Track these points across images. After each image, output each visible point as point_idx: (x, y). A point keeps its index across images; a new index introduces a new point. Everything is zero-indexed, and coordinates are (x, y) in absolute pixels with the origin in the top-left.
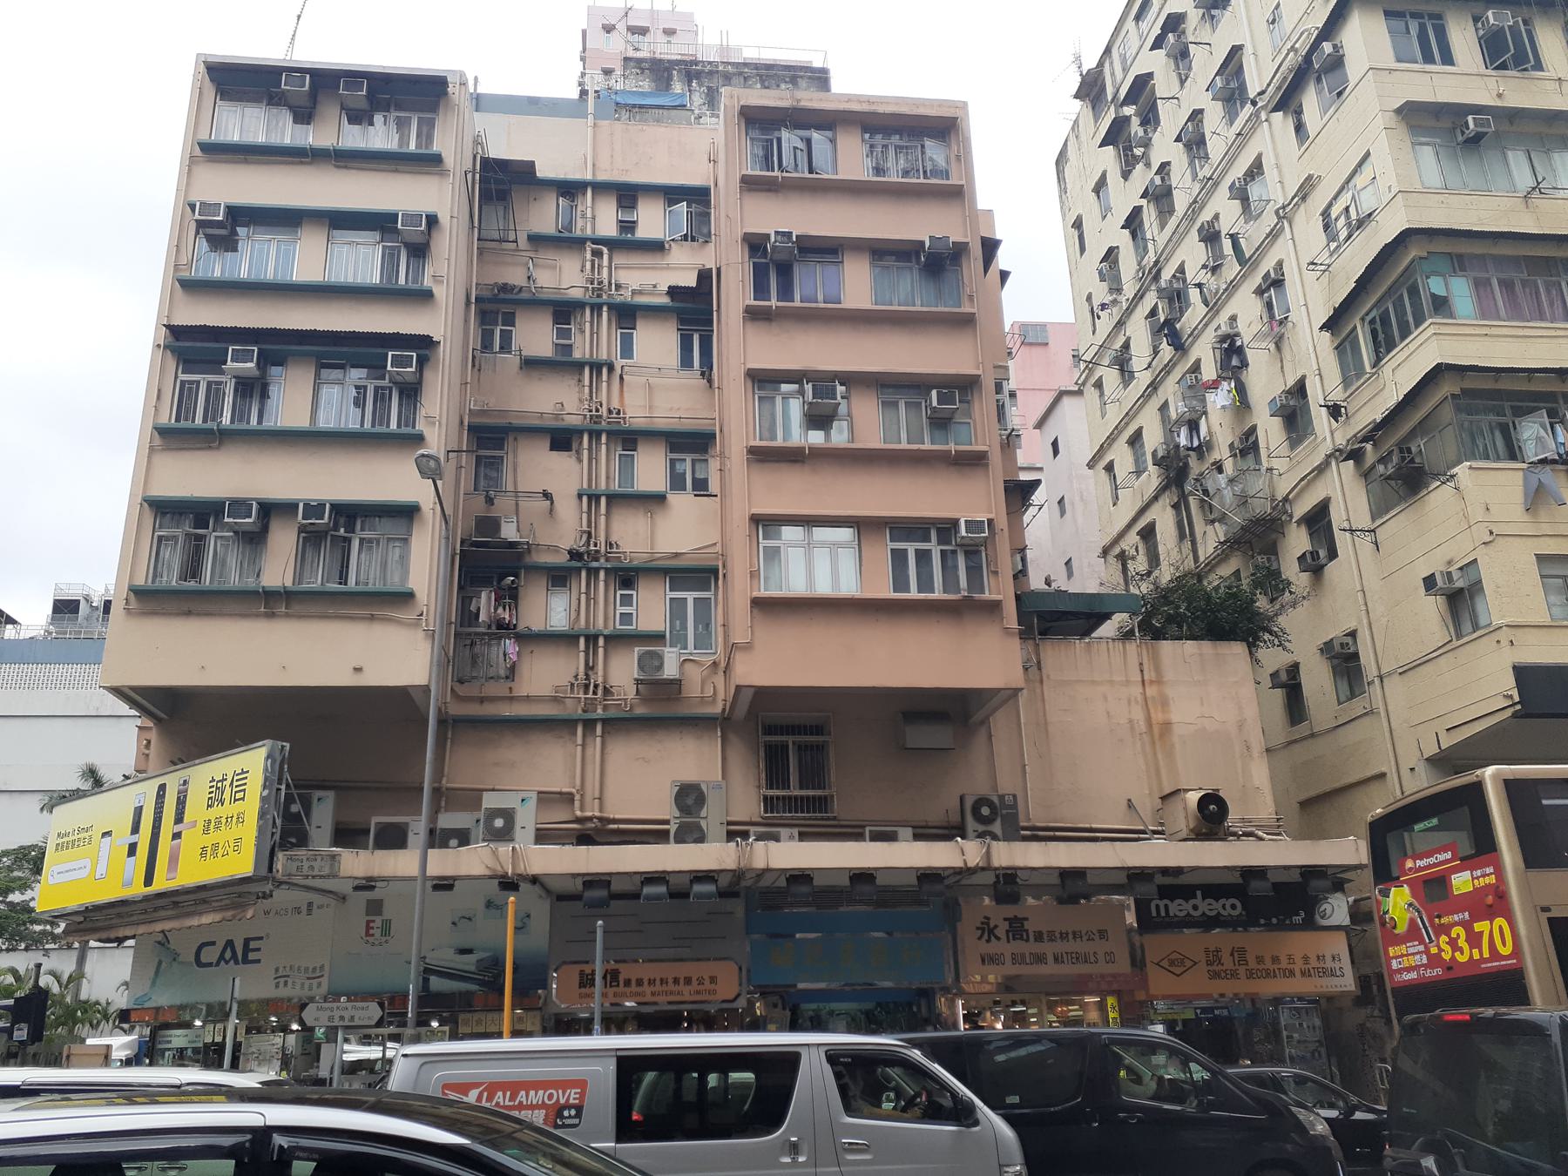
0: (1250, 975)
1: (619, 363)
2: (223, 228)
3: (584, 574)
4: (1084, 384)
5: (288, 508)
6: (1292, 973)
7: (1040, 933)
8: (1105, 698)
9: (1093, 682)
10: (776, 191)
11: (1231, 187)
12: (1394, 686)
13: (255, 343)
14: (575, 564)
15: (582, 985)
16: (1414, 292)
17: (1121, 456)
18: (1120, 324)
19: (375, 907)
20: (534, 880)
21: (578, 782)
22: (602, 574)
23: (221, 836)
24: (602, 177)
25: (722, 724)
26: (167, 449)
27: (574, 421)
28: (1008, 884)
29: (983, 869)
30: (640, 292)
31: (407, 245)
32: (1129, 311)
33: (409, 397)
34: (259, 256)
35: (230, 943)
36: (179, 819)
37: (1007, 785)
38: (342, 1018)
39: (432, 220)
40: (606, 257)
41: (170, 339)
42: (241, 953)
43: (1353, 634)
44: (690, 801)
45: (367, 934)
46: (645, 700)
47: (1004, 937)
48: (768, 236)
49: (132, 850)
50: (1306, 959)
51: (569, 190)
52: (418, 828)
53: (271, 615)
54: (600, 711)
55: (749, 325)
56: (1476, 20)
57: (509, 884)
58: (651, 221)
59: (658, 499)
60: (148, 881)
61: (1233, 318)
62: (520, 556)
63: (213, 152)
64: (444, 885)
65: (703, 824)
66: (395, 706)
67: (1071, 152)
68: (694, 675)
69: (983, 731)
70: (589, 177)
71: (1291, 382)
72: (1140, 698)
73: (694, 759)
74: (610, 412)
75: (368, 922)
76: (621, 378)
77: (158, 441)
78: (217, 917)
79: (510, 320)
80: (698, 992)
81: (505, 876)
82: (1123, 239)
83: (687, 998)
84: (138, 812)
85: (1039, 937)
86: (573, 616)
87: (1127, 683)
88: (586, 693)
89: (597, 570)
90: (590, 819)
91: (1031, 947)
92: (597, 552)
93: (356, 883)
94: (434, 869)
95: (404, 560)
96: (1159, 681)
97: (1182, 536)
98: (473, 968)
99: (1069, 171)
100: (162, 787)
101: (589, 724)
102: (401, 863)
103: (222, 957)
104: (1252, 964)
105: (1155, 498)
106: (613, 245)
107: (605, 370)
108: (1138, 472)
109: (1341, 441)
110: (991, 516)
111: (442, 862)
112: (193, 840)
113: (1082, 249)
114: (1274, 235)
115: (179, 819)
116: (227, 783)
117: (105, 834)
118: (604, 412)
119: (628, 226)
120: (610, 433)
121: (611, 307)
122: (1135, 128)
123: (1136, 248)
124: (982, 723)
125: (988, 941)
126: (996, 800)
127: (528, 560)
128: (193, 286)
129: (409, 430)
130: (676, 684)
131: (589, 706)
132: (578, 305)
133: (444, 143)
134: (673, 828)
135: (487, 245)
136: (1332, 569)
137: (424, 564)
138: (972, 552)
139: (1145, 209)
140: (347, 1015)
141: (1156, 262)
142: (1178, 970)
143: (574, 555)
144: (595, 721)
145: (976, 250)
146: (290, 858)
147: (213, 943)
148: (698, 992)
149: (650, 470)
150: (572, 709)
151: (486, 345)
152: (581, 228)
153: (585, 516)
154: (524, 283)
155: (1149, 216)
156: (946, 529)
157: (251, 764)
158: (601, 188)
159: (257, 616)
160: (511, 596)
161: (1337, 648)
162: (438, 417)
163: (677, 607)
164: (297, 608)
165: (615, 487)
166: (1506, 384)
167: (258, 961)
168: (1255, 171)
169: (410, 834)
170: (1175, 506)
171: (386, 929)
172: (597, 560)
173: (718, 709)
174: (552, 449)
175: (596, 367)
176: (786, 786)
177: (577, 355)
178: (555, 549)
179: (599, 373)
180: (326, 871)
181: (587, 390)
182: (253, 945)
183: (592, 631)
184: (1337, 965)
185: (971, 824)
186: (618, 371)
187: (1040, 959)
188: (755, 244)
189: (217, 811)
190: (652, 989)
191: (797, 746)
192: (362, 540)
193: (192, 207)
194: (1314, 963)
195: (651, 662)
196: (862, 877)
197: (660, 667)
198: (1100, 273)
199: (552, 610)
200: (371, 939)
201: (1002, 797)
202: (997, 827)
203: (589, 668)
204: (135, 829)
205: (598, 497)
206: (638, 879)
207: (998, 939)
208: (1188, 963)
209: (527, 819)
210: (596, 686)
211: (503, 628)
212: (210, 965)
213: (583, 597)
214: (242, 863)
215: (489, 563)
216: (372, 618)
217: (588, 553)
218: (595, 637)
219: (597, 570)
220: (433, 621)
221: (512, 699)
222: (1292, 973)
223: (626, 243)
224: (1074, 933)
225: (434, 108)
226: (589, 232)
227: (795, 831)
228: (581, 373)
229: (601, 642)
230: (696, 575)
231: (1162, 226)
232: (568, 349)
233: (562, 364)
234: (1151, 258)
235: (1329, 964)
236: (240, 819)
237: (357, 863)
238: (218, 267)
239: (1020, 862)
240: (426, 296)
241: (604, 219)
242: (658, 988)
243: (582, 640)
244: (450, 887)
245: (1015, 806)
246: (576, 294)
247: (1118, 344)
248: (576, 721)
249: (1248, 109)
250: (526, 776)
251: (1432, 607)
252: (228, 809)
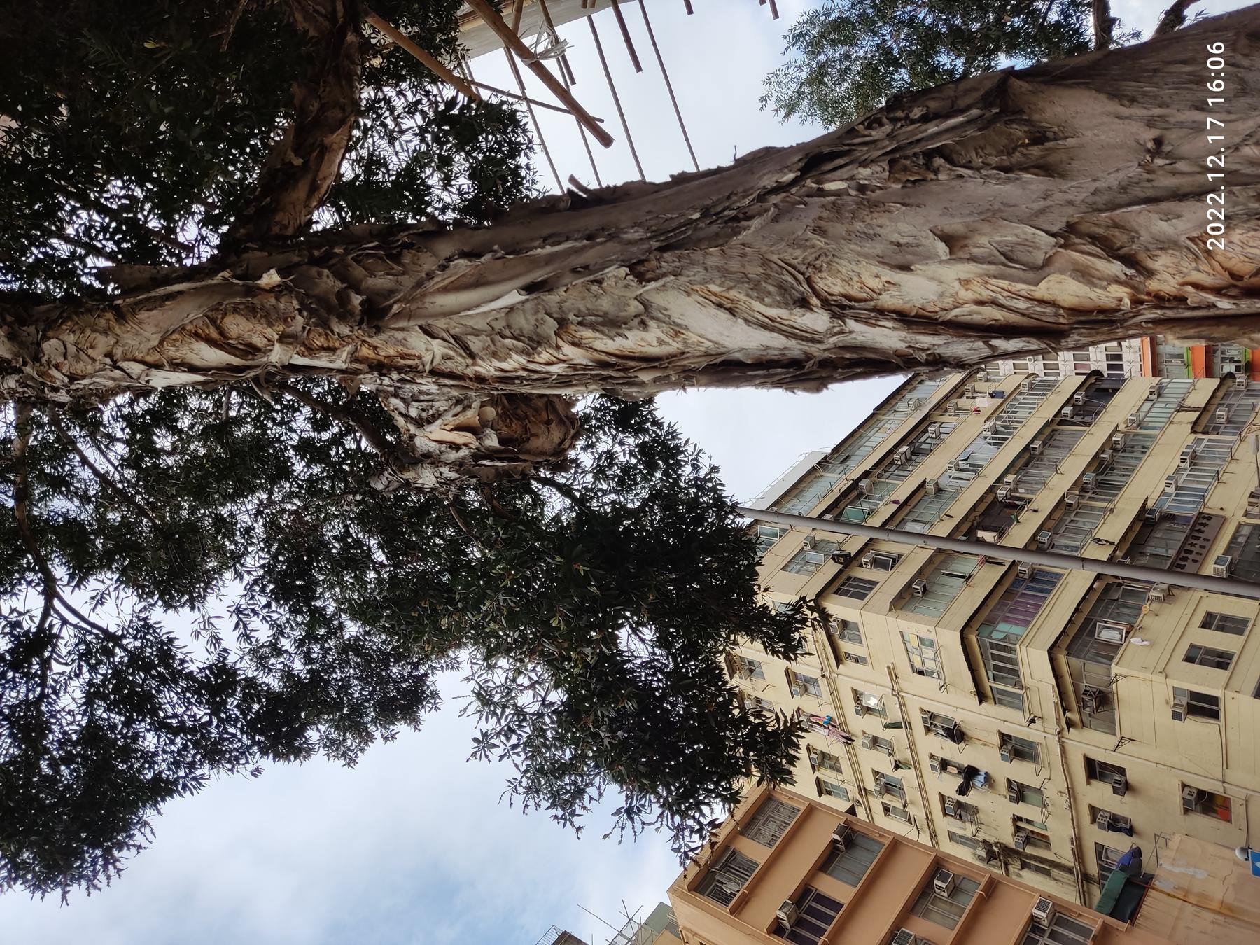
11: (858, 713)
12: (1232, 776)
16: (993, 646)
43: (1184, 786)
56: (861, 565)
61: (932, 756)
71: (997, 741)
97: (1047, 873)
109: (1053, 727)
114: (902, 705)
123: (837, 795)
136: (1131, 777)
139: (821, 777)
155: (827, 775)
161: (1192, 798)
166: (1073, 631)
168: (857, 695)
170: (1024, 866)
231: (839, 771)
249: (823, 683)
251: (1194, 726)
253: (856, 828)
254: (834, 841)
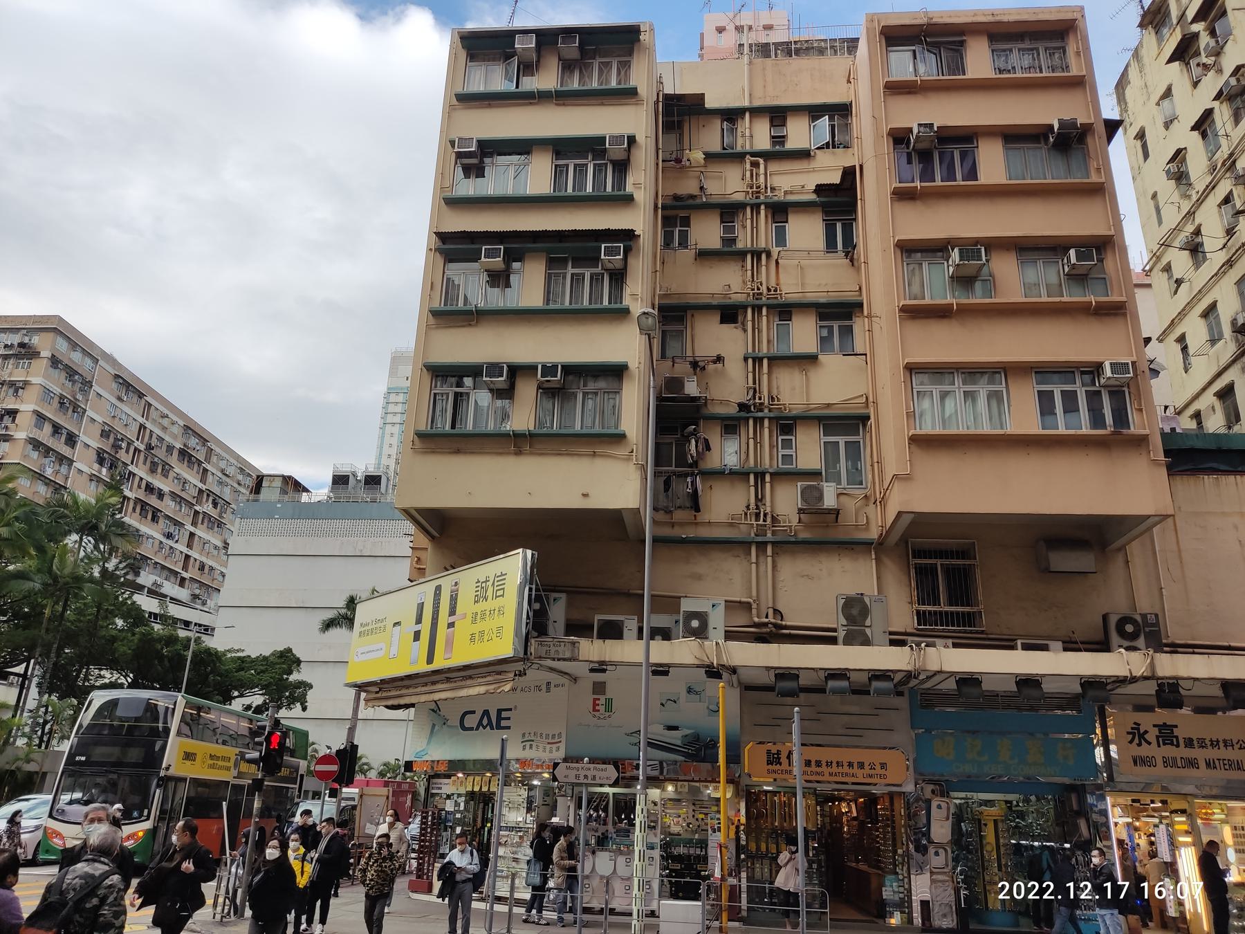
1: (775, 251)
2: (475, 158)
3: (751, 422)
4: (1151, 270)
5: (530, 369)
7: (1191, 740)
8: (1236, 527)
9: (1223, 513)
10: (915, 93)
13: (501, 243)
14: (743, 414)
15: (769, 763)
17: (1196, 330)
18: (1191, 214)
19: (599, 688)
20: (733, 670)
21: (754, 593)
22: (766, 422)
23: (488, 625)
24: (757, 103)
25: (877, 548)
26: (438, 327)
27: (740, 298)
28: (1170, 693)
29: (1146, 678)
30: (791, 193)
31: (611, 161)
32: (1200, 202)
33: (617, 280)
34: (501, 178)
35: (486, 713)
36: (452, 612)
37: (1145, 605)
38: (586, 777)
39: (632, 140)
40: (762, 167)
41: (439, 244)
42: (495, 720)
44: (855, 612)
45: (594, 710)
46: (808, 526)
48: (910, 130)
49: (417, 636)
51: (731, 116)
52: (631, 625)
53: (519, 453)
54: (769, 535)
55: (897, 205)
57: (713, 672)
58: (798, 134)
59: (812, 359)
60: (430, 660)
62: (698, 408)
63: (467, 100)
64: (661, 671)
65: (868, 631)
66: (610, 527)
67: (1133, 74)
68: (850, 505)
69: (1120, 558)
70: (746, 104)
73: (854, 576)
74: (769, 290)
75: (595, 700)
76: (777, 263)
77: (432, 320)
78: (482, 689)
79: (686, 222)
80: (871, 776)
81: (710, 666)
82: (1193, 142)
83: (826, 778)
84: (421, 607)
85: (1189, 743)
86: (743, 457)
88: (757, 519)
89: (762, 419)
90: (765, 625)
91: (1183, 752)
92: (761, 404)
93: (592, 665)
94: (654, 659)
95: (616, 412)
98: (679, 743)
99: (1129, 93)
100: (438, 588)
101: (762, 546)
102: (628, 650)
103: (480, 723)
105: (1234, 362)
106: (767, 156)
107: (764, 256)
108: (1213, 342)
110: (1134, 359)
111: (661, 652)
112: (464, 628)
113: (1146, 155)
115: (452, 612)
116: (490, 583)
117: (396, 624)
118: (764, 289)
119: (779, 140)
120: (769, 307)
121: (768, 206)
122: (1205, 40)
123: (1206, 146)
124: (1119, 550)
125: (1139, 745)
127: (705, 411)
128: (455, 203)
129: (618, 306)
130: (837, 512)
131: (761, 531)
132: (741, 206)
133: (639, 78)
134: (841, 634)
135: (673, 164)
137: (633, 410)
138: (1117, 394)
139: (1217, 111)
140: (590, 774)
141: (1231, 155)
143: (743, 407)
144: (766, 543)
145: (1101, 129)
146: (541, 644)
147: (473, 712)
148: (871, 776)
149: (804, 334)
150: (746, 531)
151: (668, 243)
152: (742, 145)
153: (750, 375)
154: (696, 192)
156: (1095, 369)
157: (513, 566)
158: (756, 112)
159: (509, 454)
162: (638, 295)
163: (830, 452)
165: (775, 351)
167: (509, 728)
169: (625, 630)
171: (609, 704)
172: (761, 410)
173: (874, 534)
174: (722, 322)
175: (756, 254)
176: (936, 602)
177: (740, 245)
179: (759, 259)
180: (568, 655)
181: (749, 273)
182: (504, 714)
183: (759, 469)
185: (1115, 638)
186: (775, 256)
188: (899, 138)
189: (483, 605)
190: (829, 769)
191: (948, 569)
192: (585, 394)
193: (452, 143)
195: (812, 496)
196: (1028, 683)
197: (821, 498)
198: (1168, 172)
199: (728, 453)
200: (597, 714)
201: (1144, 616)
203: (759, 500)
204: (419, 621)
205: (761, 360)
206: (822, 675)
207: (1149, 743)
209: (718, 621)
210: (765, 515)
212: (471, 729)
213: (751, 441)
214: (504, 646)
215: (677, 418)
216: (594, 455)
217: (754, 404)
218: (763, 474)
219: (762, 419)
220: (638, 456)
223: (779, 154)
224: (1225, 741)
225: (630, 53)
226: (748, 148)
227: (950, 642)
228: (744, 260)
229: (768, 478)
230: (848, 423)
232: (733, 241)
233: (728, 253)
234: (1224, 152)
236: (501, 611)
237: (592, 649)
238: (469, 187)
239: (1183, 673)
240: (628, 200)
241: (759, 135)
242: (834, 769)
243: (752, 477)
244: (666, 673)
245: (1157, 624)
246: (740, 197)
247: (1190, 228)
248: (750, 543)
250: (714, 588)
252: (491, 604)
253: (1089, 140)
254: (1051, 127)
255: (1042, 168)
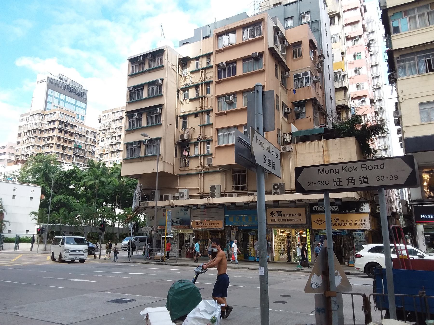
0: (340, 224)
6: (352, 224)
8: (313, 156)
47: (276, 215)
50: (356, 221)
51: (197, 59)
52: (170, 196)
72: (322, 155)
85: (284, 215)
87: (319, 152)
91: (282, 217)
96: (328, 150)
101: (201, 174)
104: (340, 222)
126: (279, 184)
134: (210, 194)
142: (320, 223)
143: (198, 139)
158: (203, 56)
160: (188, 149)
164: (145, 159)
165: (206, 123)
174: (195, 117)
178: (195, 139)
184: (365, 222)
185: (273, 191)
187: (284, 220)
194: (358, 222)
201: (280, 184)
202: (278, 191)
208: (323, 222)
211: (189, 157)
221: (189, 170)
222: (352, 224)
235: (363, 222)
255: (252, 67)
